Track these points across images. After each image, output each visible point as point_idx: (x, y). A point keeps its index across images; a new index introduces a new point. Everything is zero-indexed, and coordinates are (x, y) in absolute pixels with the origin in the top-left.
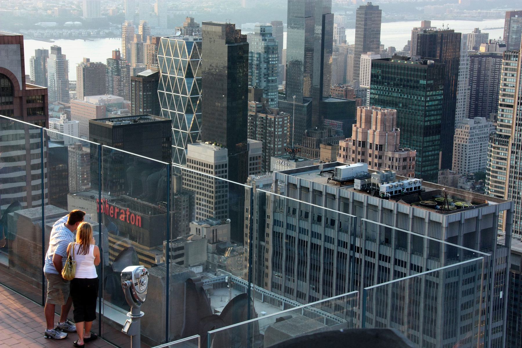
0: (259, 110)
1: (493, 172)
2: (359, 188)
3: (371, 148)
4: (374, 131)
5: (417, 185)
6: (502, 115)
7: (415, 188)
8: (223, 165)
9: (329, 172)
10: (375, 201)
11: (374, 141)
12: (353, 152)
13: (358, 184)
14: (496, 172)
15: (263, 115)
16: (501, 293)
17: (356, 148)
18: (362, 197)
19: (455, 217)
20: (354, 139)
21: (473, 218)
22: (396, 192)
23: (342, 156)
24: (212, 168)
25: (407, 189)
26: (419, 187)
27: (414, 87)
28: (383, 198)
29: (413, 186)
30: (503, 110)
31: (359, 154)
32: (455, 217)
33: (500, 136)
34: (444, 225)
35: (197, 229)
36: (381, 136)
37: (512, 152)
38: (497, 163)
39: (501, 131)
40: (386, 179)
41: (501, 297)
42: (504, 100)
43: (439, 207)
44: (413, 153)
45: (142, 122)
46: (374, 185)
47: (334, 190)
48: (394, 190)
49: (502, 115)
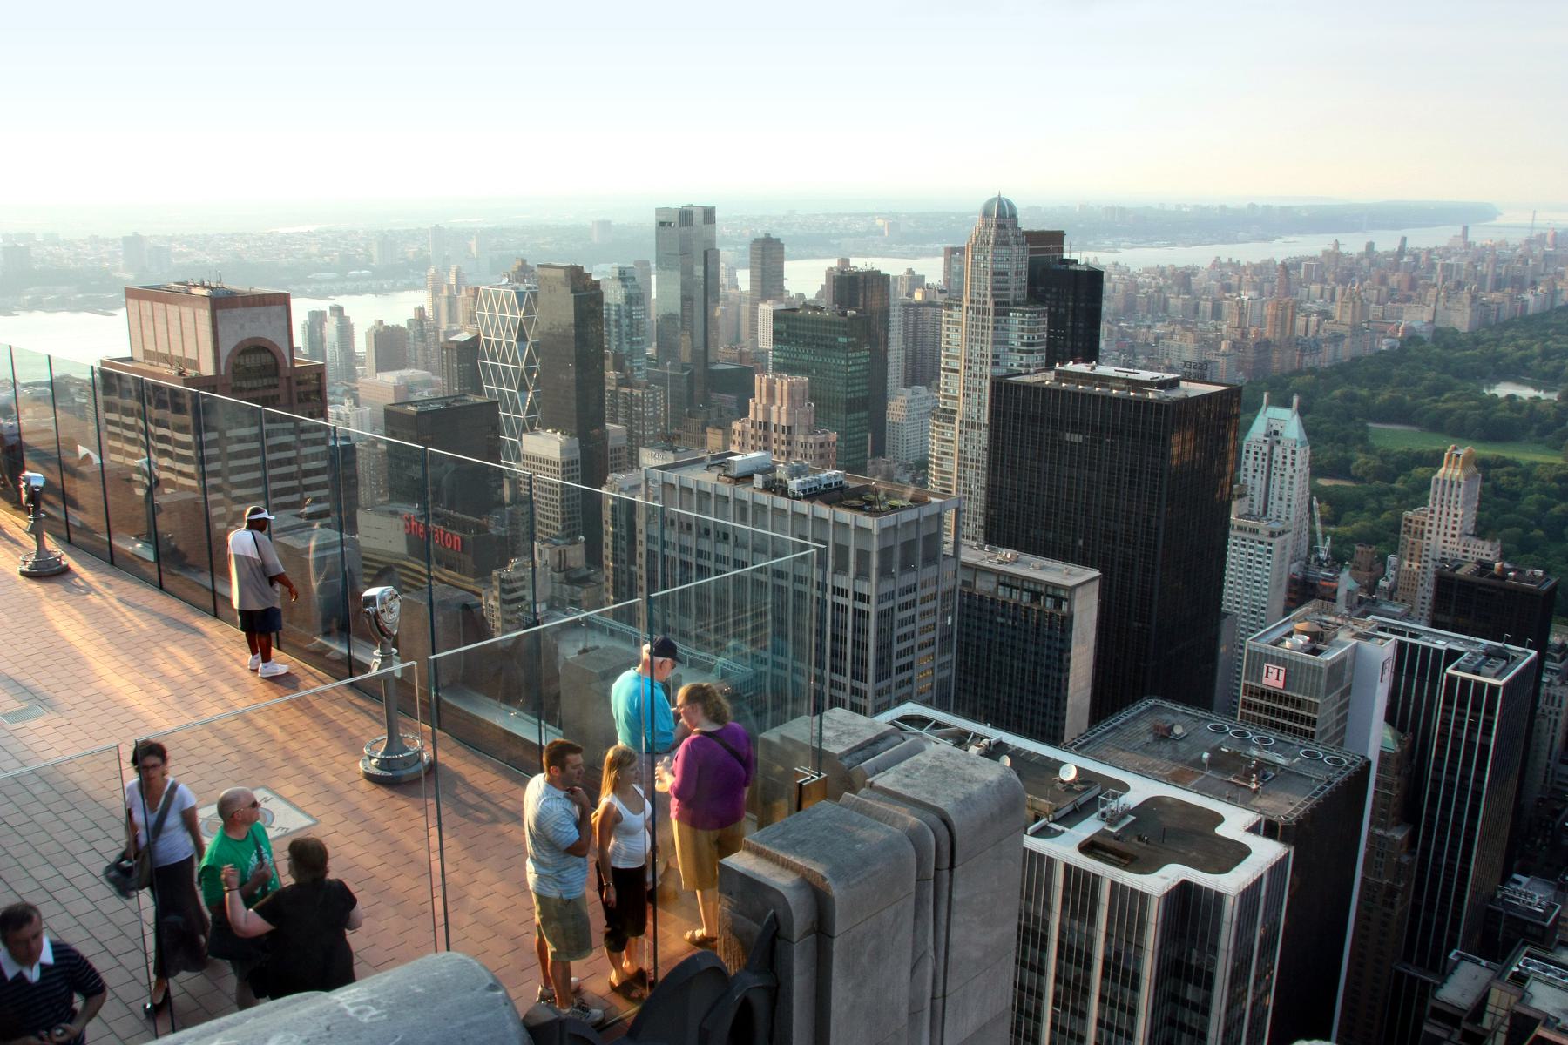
0: (621, 383)
1: (937, 458)
2: (761, 486)
3: (775, 431)
4: (779, 408)
5: (839, 479)
6: (946, 383)
7: (836, 484)
9: (719, 465)
10: (783, 503)
11: (779, 421)
13: (758, 480)
14: (941, 459)
15: (627, 390)
16: (949, 618)
18: (765, 498)
19: (889, 520)
21: (912, 521)
22: (810, 489)
25: (825, 486)
26: (841, 482)
27: (831, 347)
28: (794, 498)
29: (833, 481)
30: (946, 377)
31: (760, 439)
32: (889, 520)
33: (945, 410)
34: (875, 532)
36: (788, 413)
37: (961, 432)
38: (942, 447)
39: (945, 404)
40: (796, 472)
41: (949, 623)
42: (947, 363)
43: (868, 508)
44: (833, 436)
45: (457, 405)
46: (781, 481)
47: (727, 490)
48: (807, 487)
49: (946, 383)
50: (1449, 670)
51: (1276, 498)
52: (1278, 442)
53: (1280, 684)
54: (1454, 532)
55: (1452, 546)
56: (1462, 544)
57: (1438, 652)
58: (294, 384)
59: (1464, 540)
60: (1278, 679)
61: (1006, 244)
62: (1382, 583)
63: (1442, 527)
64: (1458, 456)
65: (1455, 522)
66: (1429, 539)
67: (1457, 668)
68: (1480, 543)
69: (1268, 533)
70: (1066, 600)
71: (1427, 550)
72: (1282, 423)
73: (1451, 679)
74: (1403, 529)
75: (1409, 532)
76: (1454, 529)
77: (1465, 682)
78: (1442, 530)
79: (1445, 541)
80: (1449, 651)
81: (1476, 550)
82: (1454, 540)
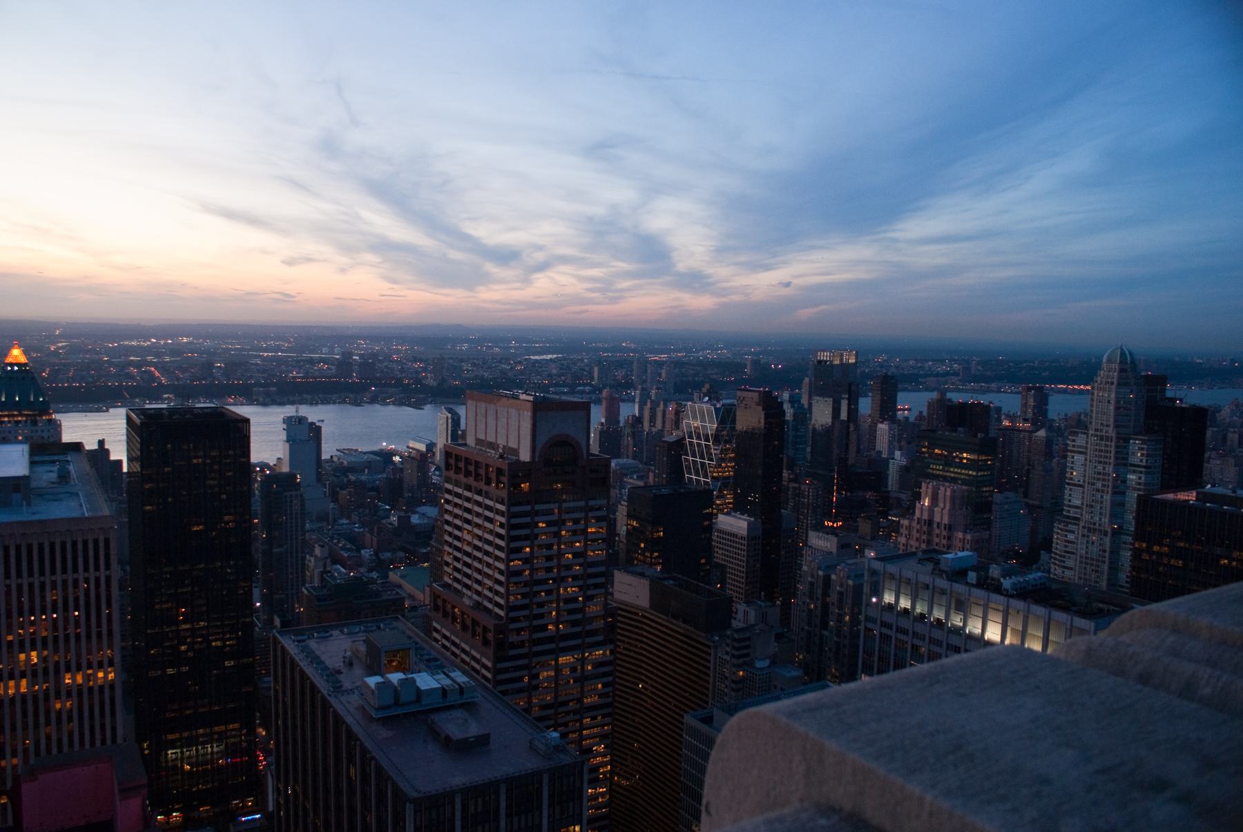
1: (1060, 555)
4: (943, 509)
5: (1043, 581)
6: (1070, 495)
7: (1041, 584)
8: (756, 537)
9: (928, 560)
11: (942, 519)
12: (918, 531)
13: (972, 576)
14: (1064, 557)
15: (796, 485)
17: (921, 527)
20: (919, 517)
23: (904, 535)
24: (745, 540)
25: (1032, 586)
26: (1045, 583)
29: (1039, 582)
33: (1068, 517)
35: (745, 611)
36: (950, 515)
37: (1083, 536)
38: (1066, 546)
39: (1069, 511)
46: (993, 579)
49: (1070, 495)
58: (1070, 555)
61: (1127, 384)
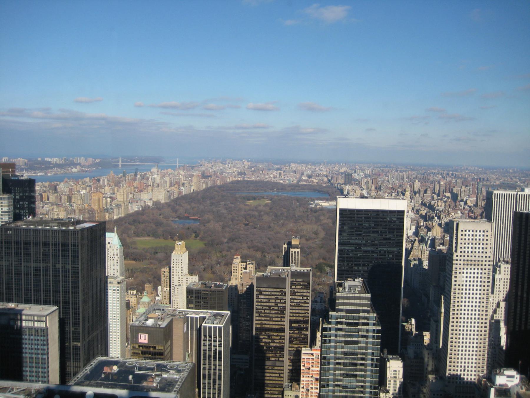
50: (203, 324)
51: (112, 269)
52: (110, 247)
53: (146, 341)
54: (182, 274)
55: (182, 279)
56: (185, 278)
57: (196, 318)
59: (185, 277)
60: (145, 339)
62: (157, 298)
63: (178, 272)
64: (180, 245)
65: (182, 270)
66: (173, 278)
67: (206, 323)
68: (191, 277)
69: (116, 283)
70: (44, 322)
71: (173, 282)
72: (111, 239)
73: (205, 328)
74: (162, 276)
75: (165, 276)
76: (182, 273)
77: (210, 328)
78: (177, 274)
79: (179, 278)
80: (200, 317)
81: (191, 280)
82: (182, 277)
